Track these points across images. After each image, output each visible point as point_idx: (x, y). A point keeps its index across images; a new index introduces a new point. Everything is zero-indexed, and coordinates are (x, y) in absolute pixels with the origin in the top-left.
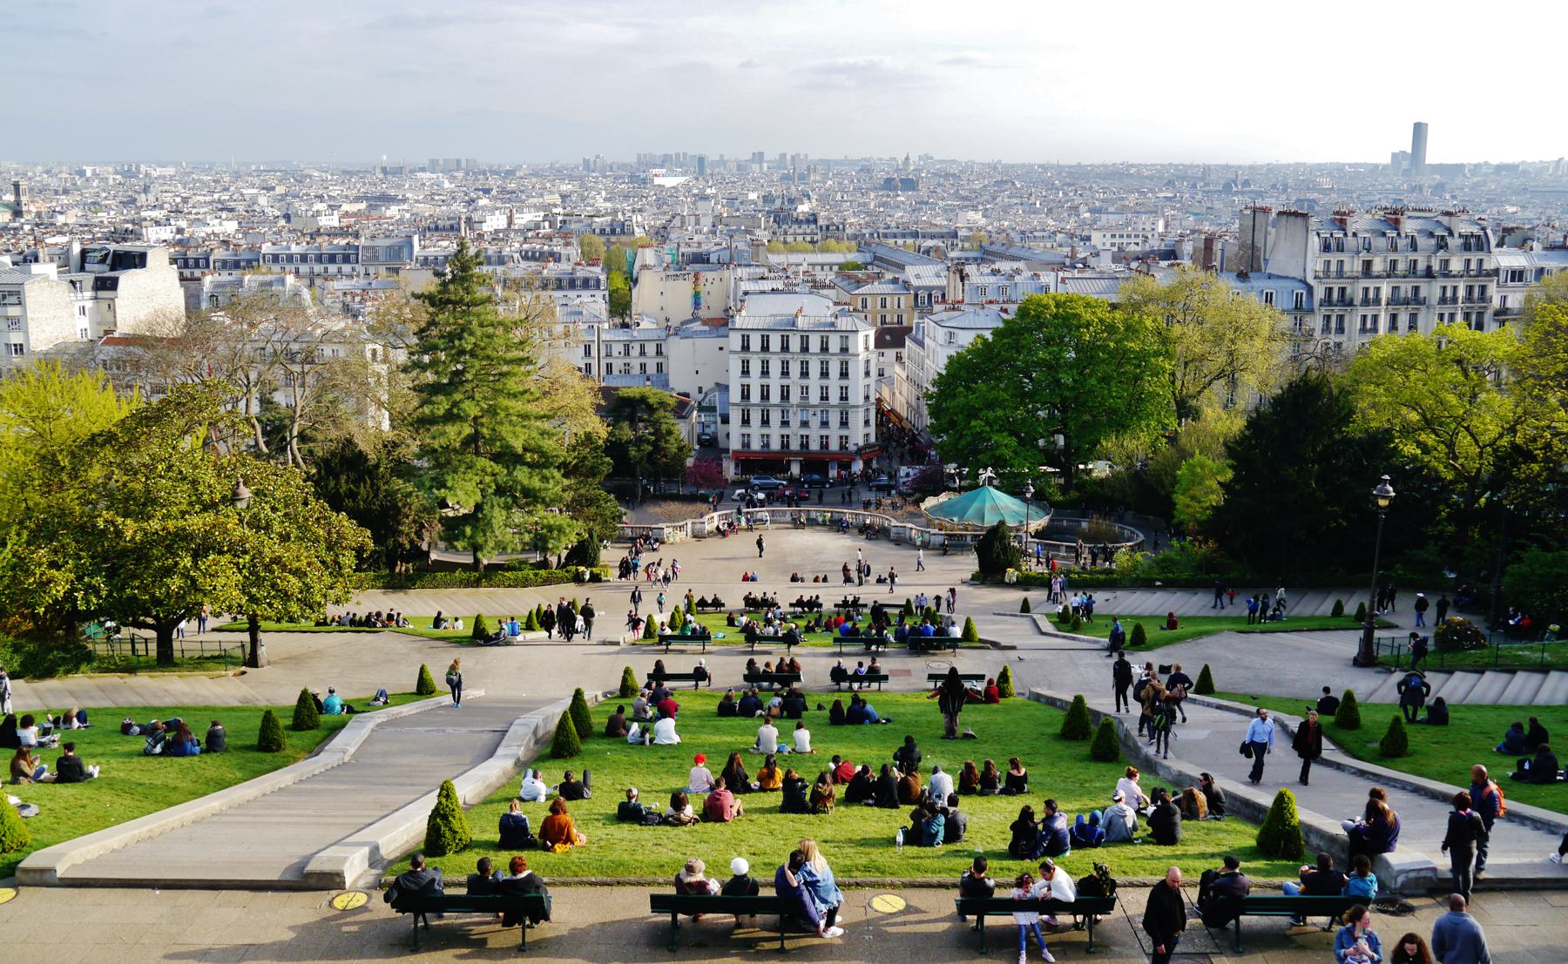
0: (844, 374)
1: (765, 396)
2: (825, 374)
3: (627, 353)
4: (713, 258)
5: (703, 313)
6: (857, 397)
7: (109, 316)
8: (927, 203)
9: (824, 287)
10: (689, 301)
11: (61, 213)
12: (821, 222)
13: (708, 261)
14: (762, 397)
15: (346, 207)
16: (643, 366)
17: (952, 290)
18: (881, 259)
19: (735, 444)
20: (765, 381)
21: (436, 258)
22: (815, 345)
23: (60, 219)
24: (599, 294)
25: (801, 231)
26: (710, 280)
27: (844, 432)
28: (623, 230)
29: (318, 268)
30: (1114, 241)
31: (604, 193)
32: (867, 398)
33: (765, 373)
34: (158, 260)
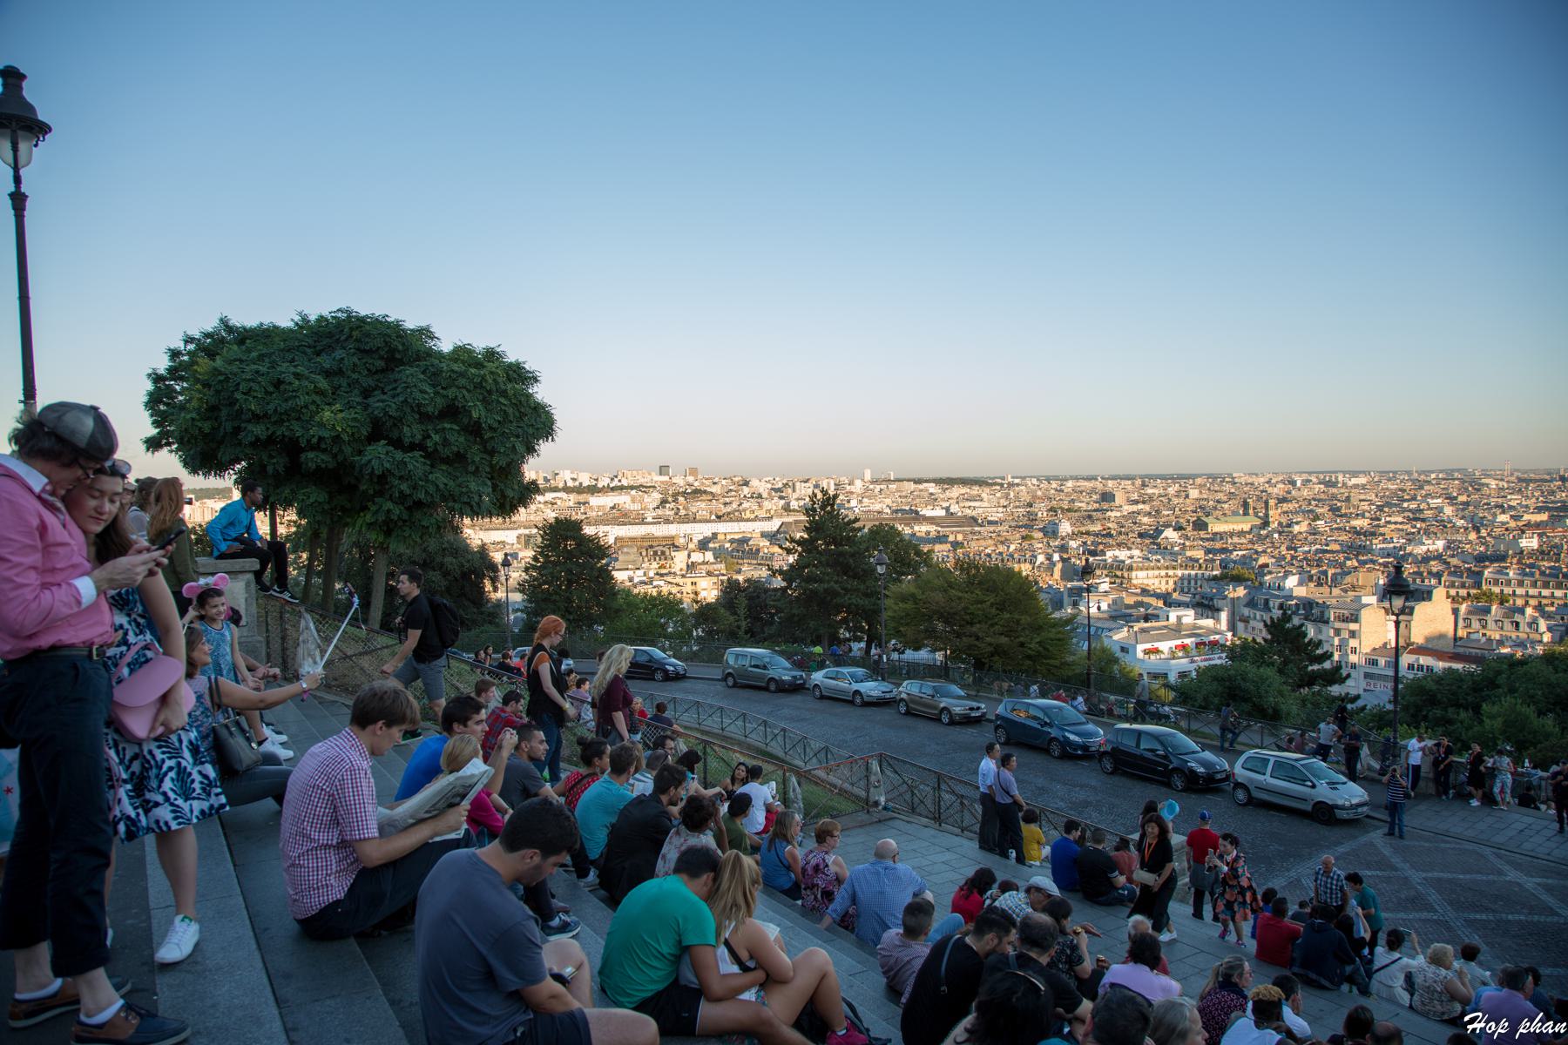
7: (1406, 632)
11: (1297, 523)
15: (1526, 517)
23: (1296, 529)
29: (1532, 592)
34: (1439, 593)
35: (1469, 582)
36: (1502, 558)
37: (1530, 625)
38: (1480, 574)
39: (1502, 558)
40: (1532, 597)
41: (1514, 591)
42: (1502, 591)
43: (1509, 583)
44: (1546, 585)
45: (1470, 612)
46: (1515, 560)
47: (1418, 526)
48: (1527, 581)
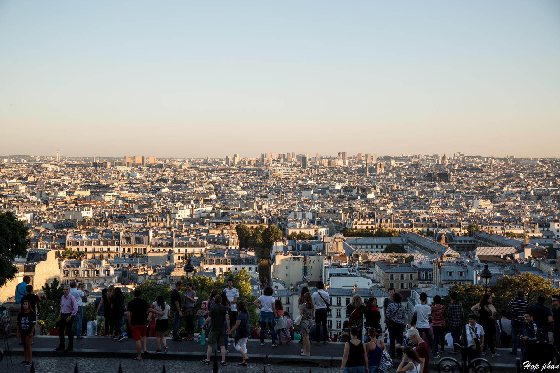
4: (314, 247)
5: (308, 278)
8: (454, 192)
9: (368, 273)
10: (301, 272)
13: (311, 249)
14: (337, 327)
15: (76, 193)
17: (435, 272)
18: (412, 242)
20: (338, 319)
24: (254, 267)
25: (365, 222)
26: (312, 261)
29: (97, 248)
31: (241, 184)
33: (339, 315)
34: (51, 254)
35: (57, 244)
36: (71, 225)
37: (105, 271)
38: (63, 237)
39: (71, 225)
40: (97, 252)
41: (86, 249)
42: (78, 249)
43: (82, 243)
44: (105, 244)
45: (67, 266)
46: (81, 227)
47: (3, 201)
48: (94, 241)
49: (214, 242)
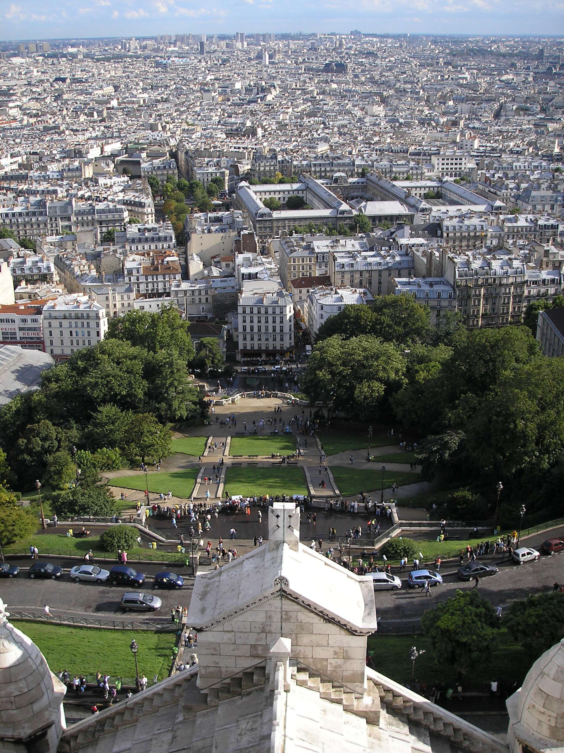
0: (282, 322)
1: (252, 329)
2: (274, 322)
3: (193, 294)
6: (286, 330)
12: (280, 158)
16: (200, 299)
18: (311, 189)
19: (241, 347)
20: (252, 324)
21: (85, 211)
22: (270, 311)
27: (282, 343)
28: (170, 167)
30: (443, 162)
32: (290, 330)
49: (132, 205)
